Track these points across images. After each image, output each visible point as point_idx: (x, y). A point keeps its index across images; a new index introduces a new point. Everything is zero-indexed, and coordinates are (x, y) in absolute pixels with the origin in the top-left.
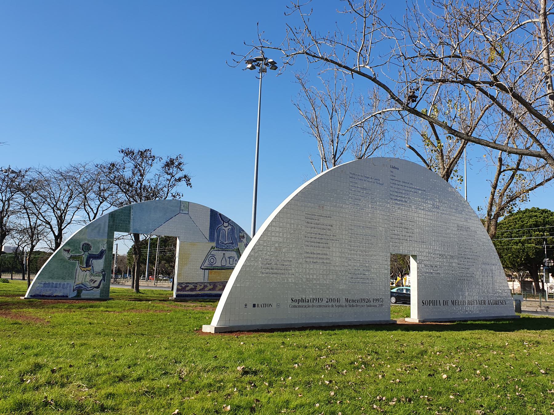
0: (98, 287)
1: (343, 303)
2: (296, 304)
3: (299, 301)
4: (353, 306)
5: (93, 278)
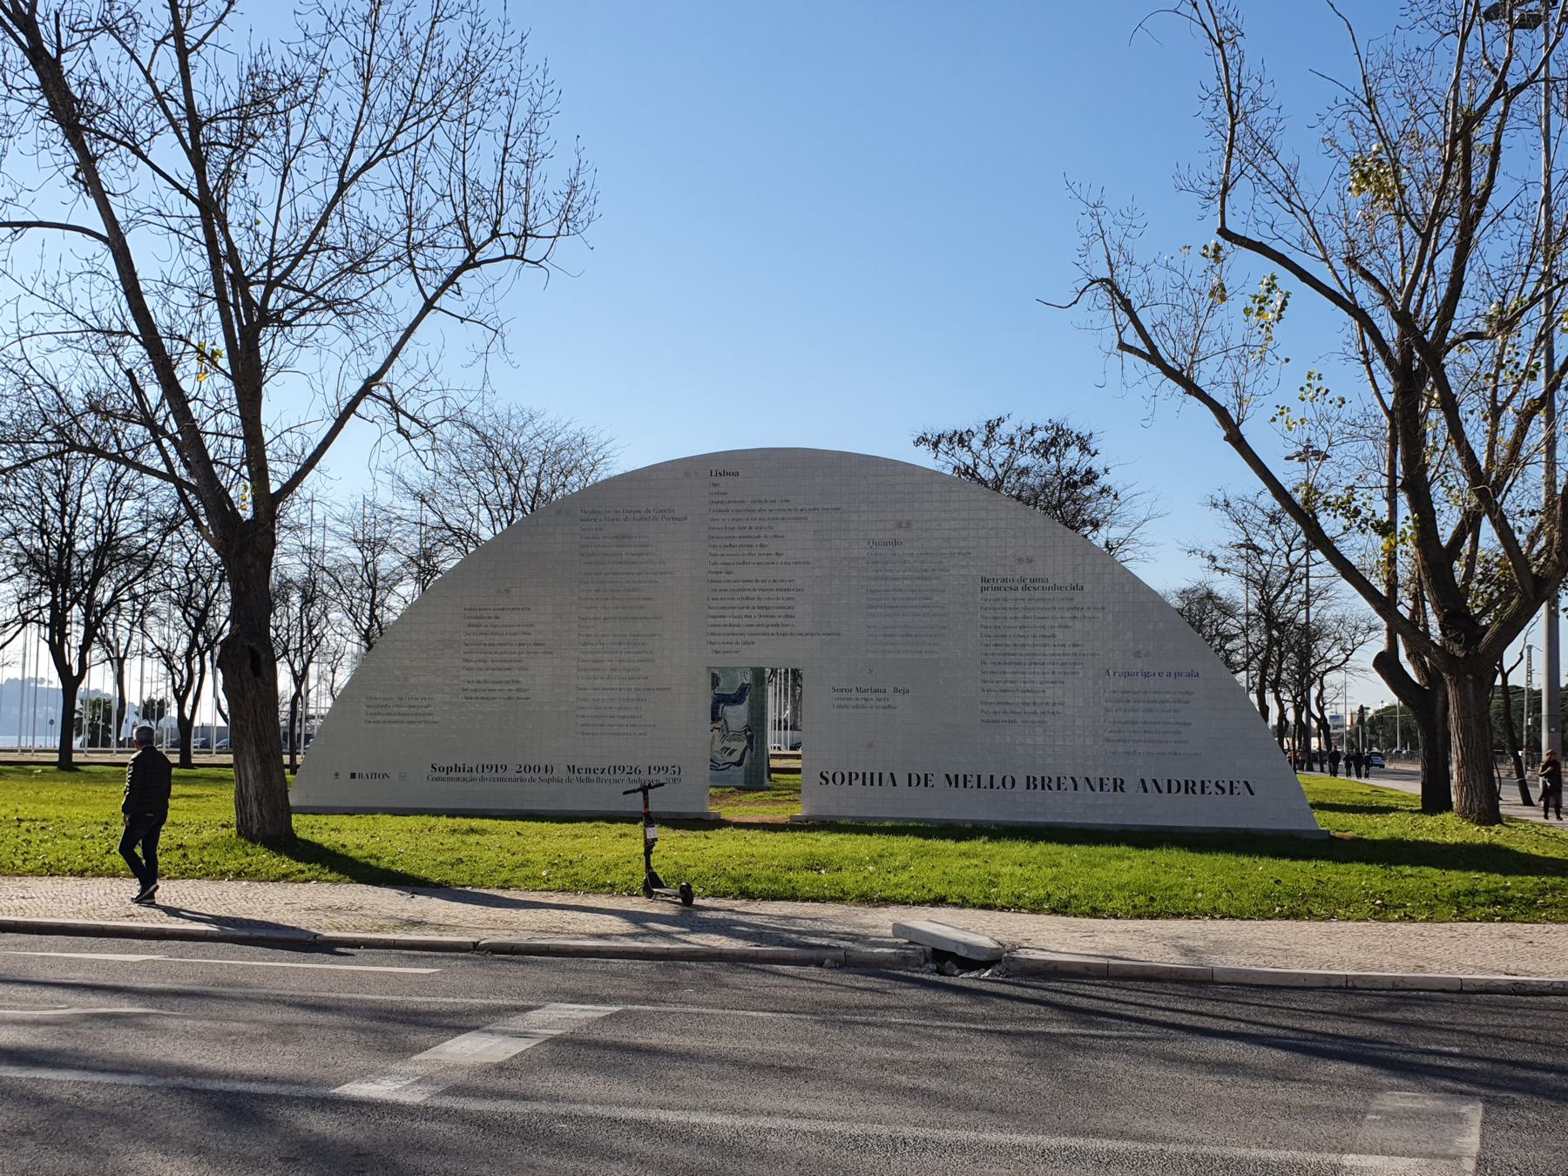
0: (739, 764)
1: (561, 772)
2: (443, 774)
3: (449, 770)
4: (588, 780)
5: (727, 744)
